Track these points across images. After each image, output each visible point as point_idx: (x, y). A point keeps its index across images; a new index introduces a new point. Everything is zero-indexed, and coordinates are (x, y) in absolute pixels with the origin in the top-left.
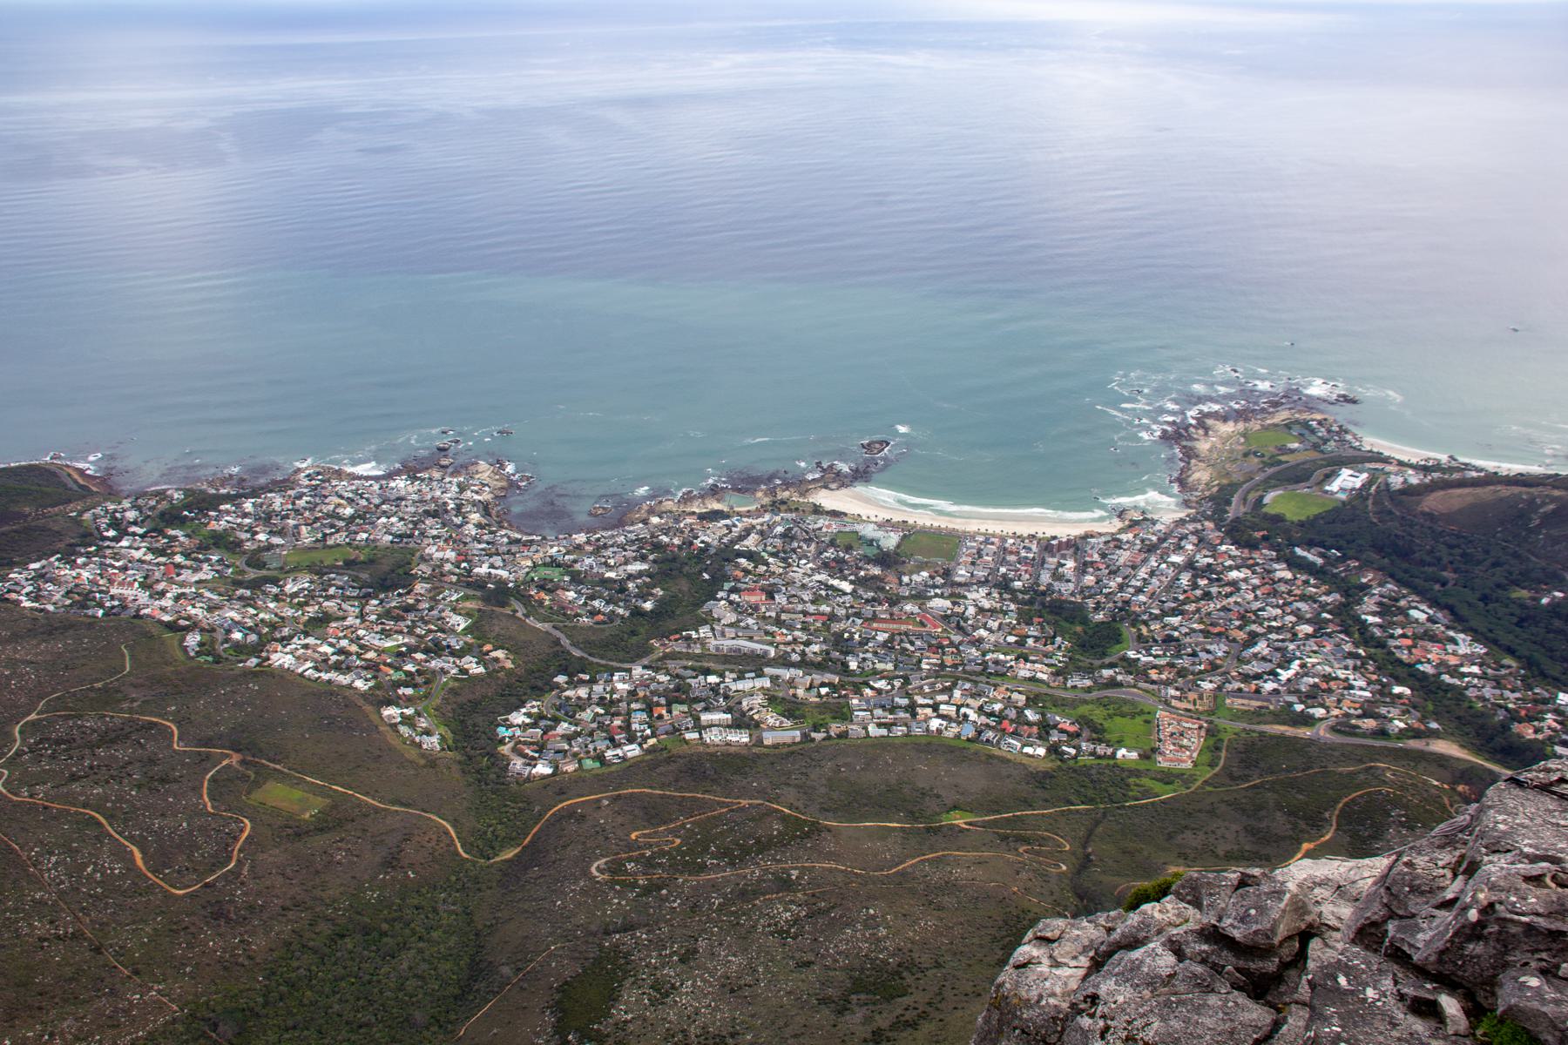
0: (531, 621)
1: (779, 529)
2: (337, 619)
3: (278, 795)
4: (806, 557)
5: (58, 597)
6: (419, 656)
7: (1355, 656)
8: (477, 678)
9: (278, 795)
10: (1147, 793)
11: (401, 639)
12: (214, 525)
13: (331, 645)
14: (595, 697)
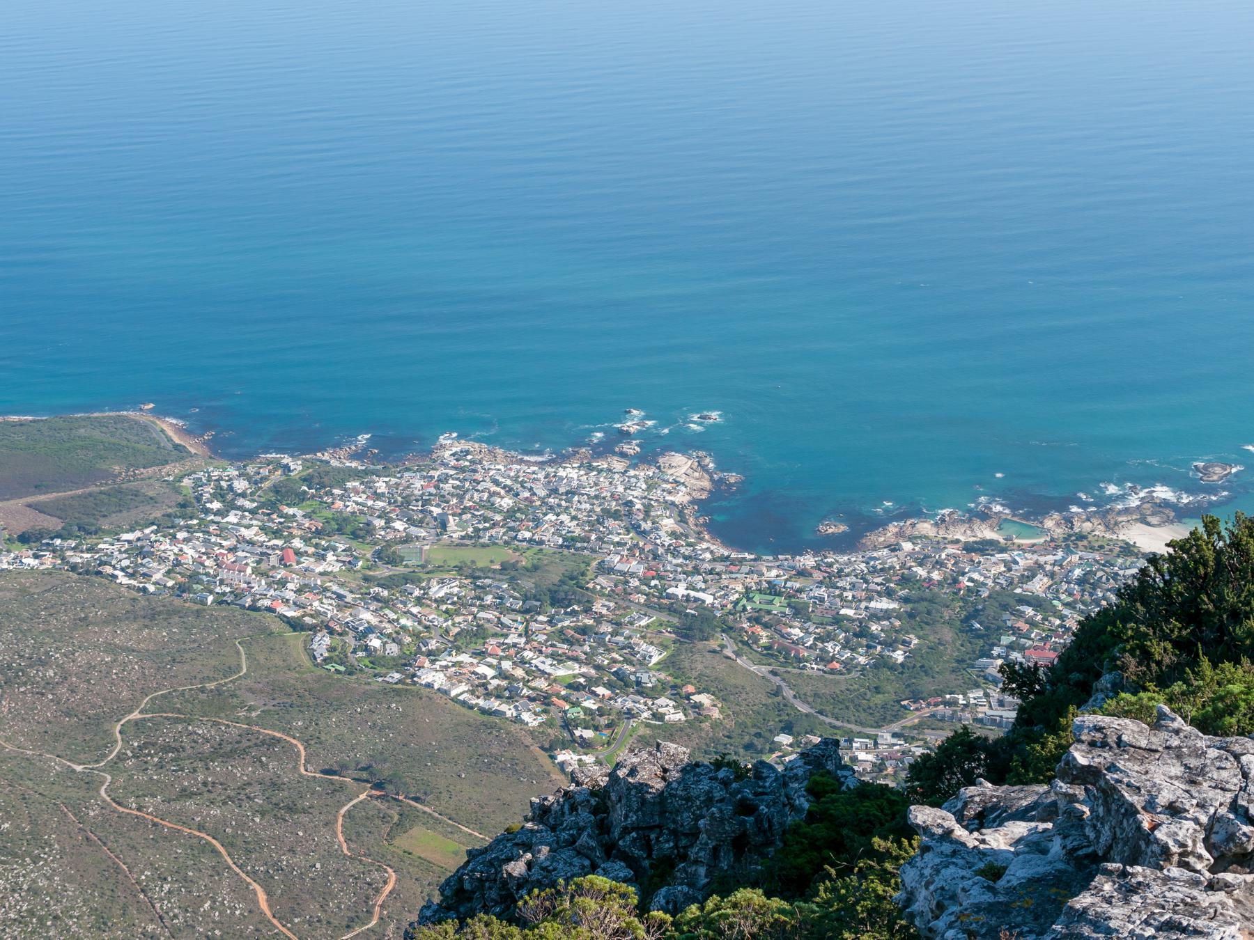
2: (495, 635)
5: (157, 577)
6: (601, 691)
8: (673, 725)
11: (576, 669)
12: (339, 504)
13: (490, 666)
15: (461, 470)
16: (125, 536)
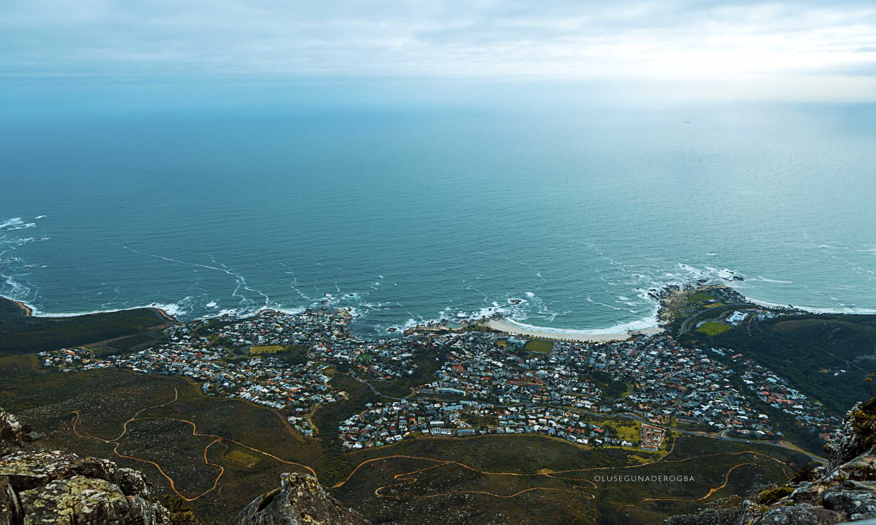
0: (357, 378)
1: (471, 338)
3: (238, 456)
5: (149, 366)
6: (306, 394)
7: (742, 399)
9: (238, 456)
10: (636, 462)
11: (300, 386)
14: (384, 414)
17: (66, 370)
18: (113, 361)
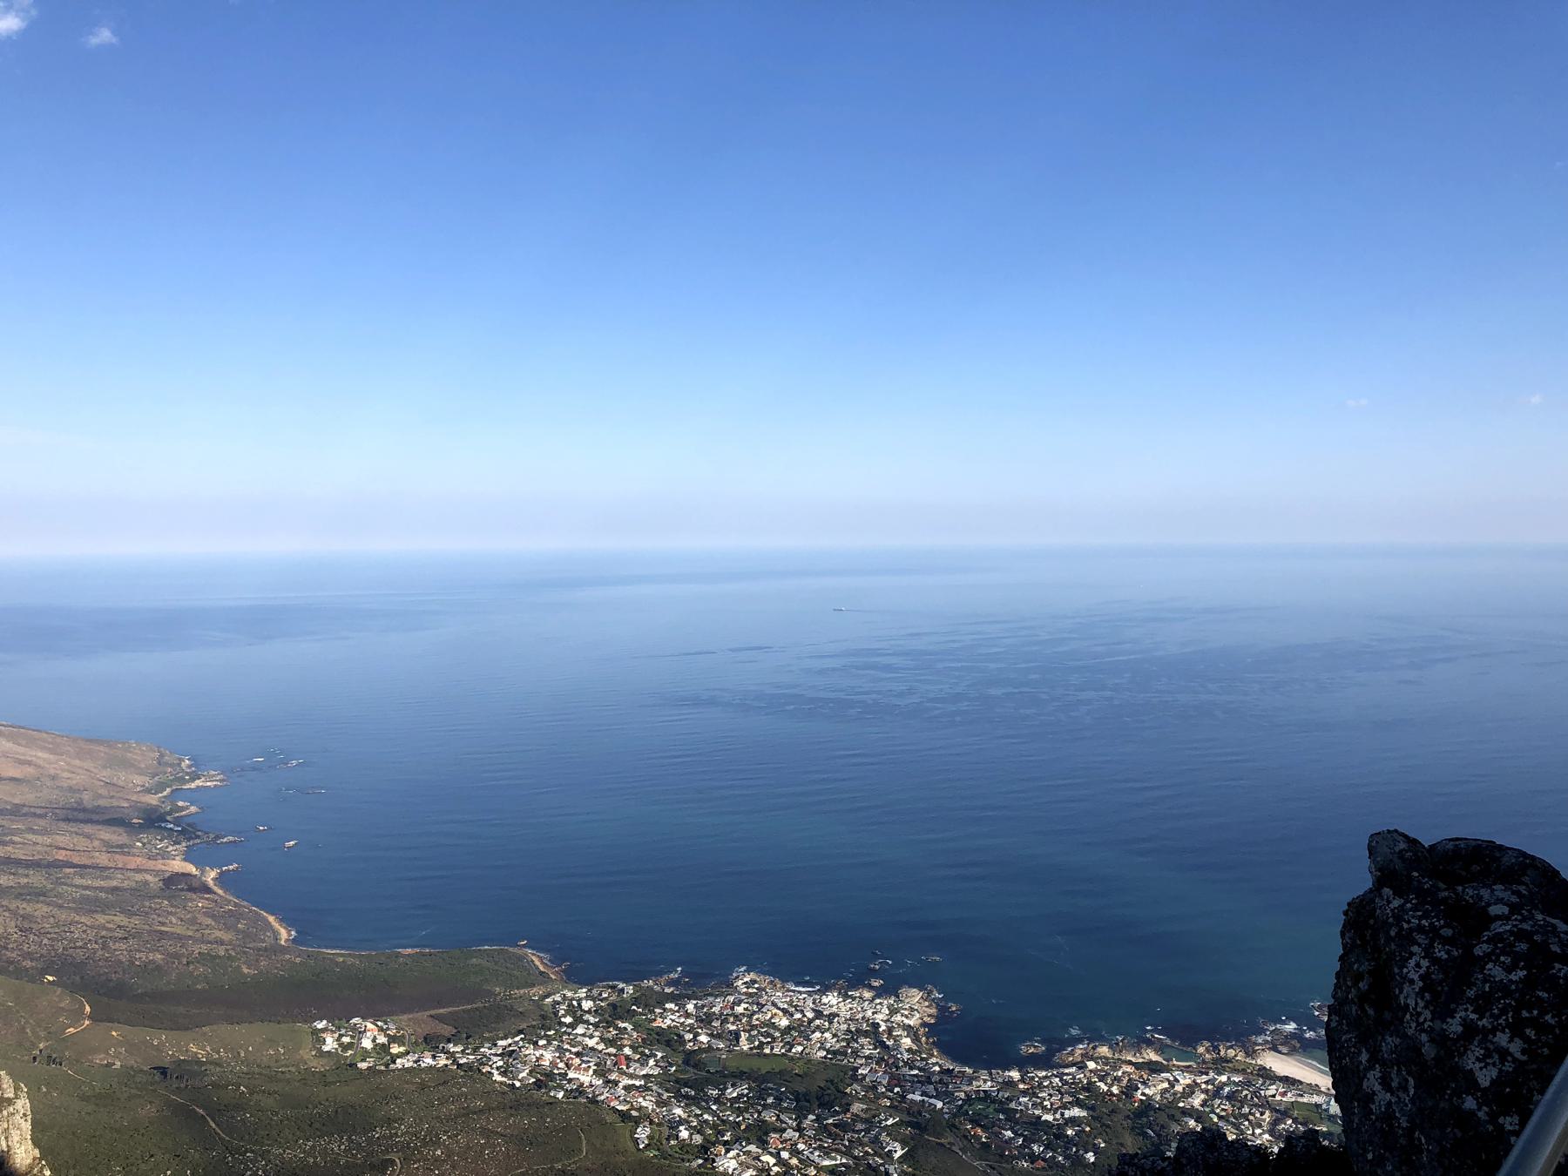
2: (776, 1130)
4: (1260, 1126)
12: (659, 1023)
15: (750, 995)
16: (501, 1043)
17: (363, 1065)
18: (451, 1055)
